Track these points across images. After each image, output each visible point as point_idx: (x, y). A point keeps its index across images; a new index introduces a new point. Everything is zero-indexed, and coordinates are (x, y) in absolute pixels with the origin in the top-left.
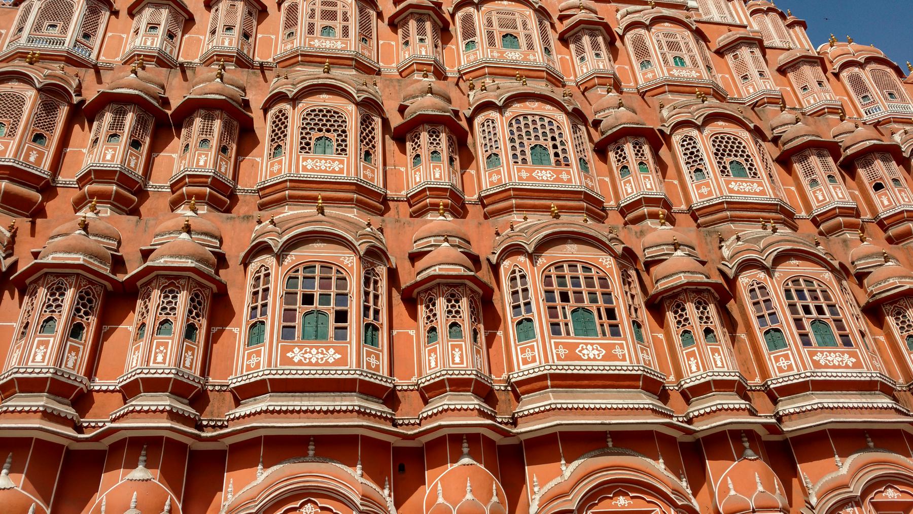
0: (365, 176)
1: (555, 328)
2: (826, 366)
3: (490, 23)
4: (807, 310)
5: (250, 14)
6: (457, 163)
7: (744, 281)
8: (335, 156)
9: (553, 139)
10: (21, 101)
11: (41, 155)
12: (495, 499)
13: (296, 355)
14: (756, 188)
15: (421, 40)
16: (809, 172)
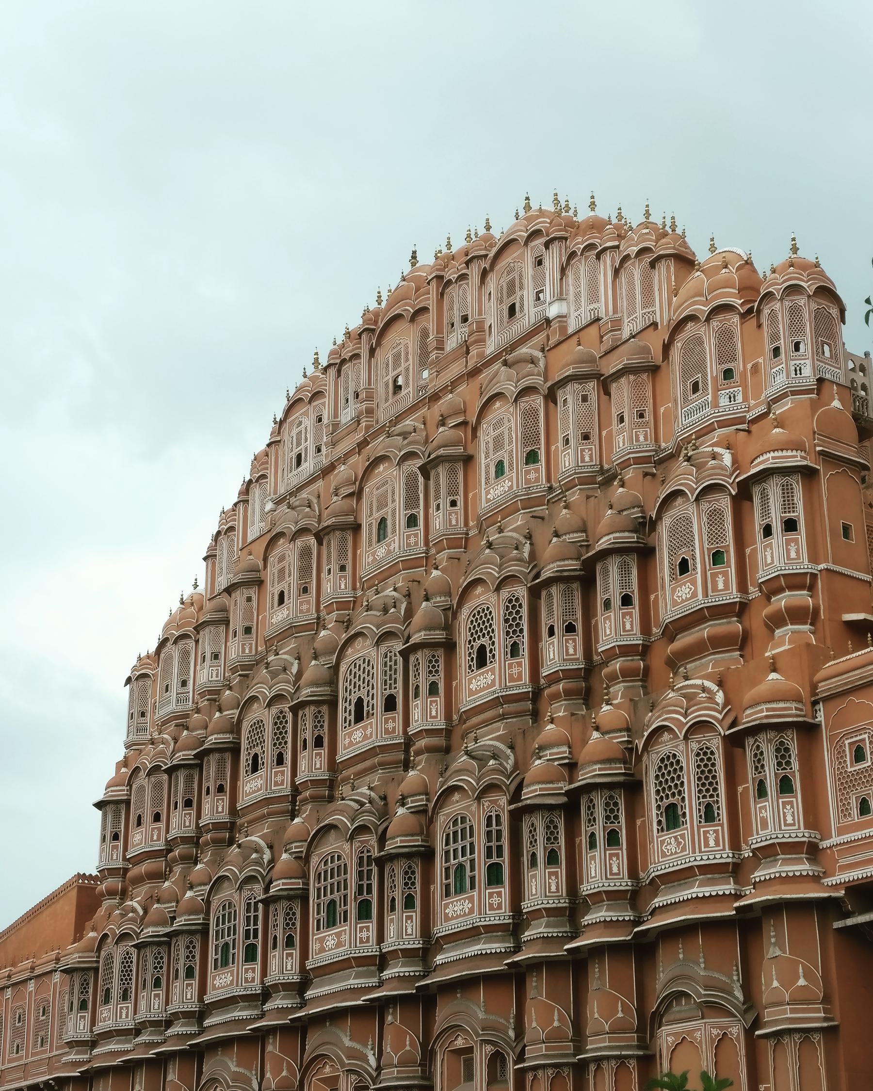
11: (159, 829)
12: (284, 1073)
14: (490, 677)
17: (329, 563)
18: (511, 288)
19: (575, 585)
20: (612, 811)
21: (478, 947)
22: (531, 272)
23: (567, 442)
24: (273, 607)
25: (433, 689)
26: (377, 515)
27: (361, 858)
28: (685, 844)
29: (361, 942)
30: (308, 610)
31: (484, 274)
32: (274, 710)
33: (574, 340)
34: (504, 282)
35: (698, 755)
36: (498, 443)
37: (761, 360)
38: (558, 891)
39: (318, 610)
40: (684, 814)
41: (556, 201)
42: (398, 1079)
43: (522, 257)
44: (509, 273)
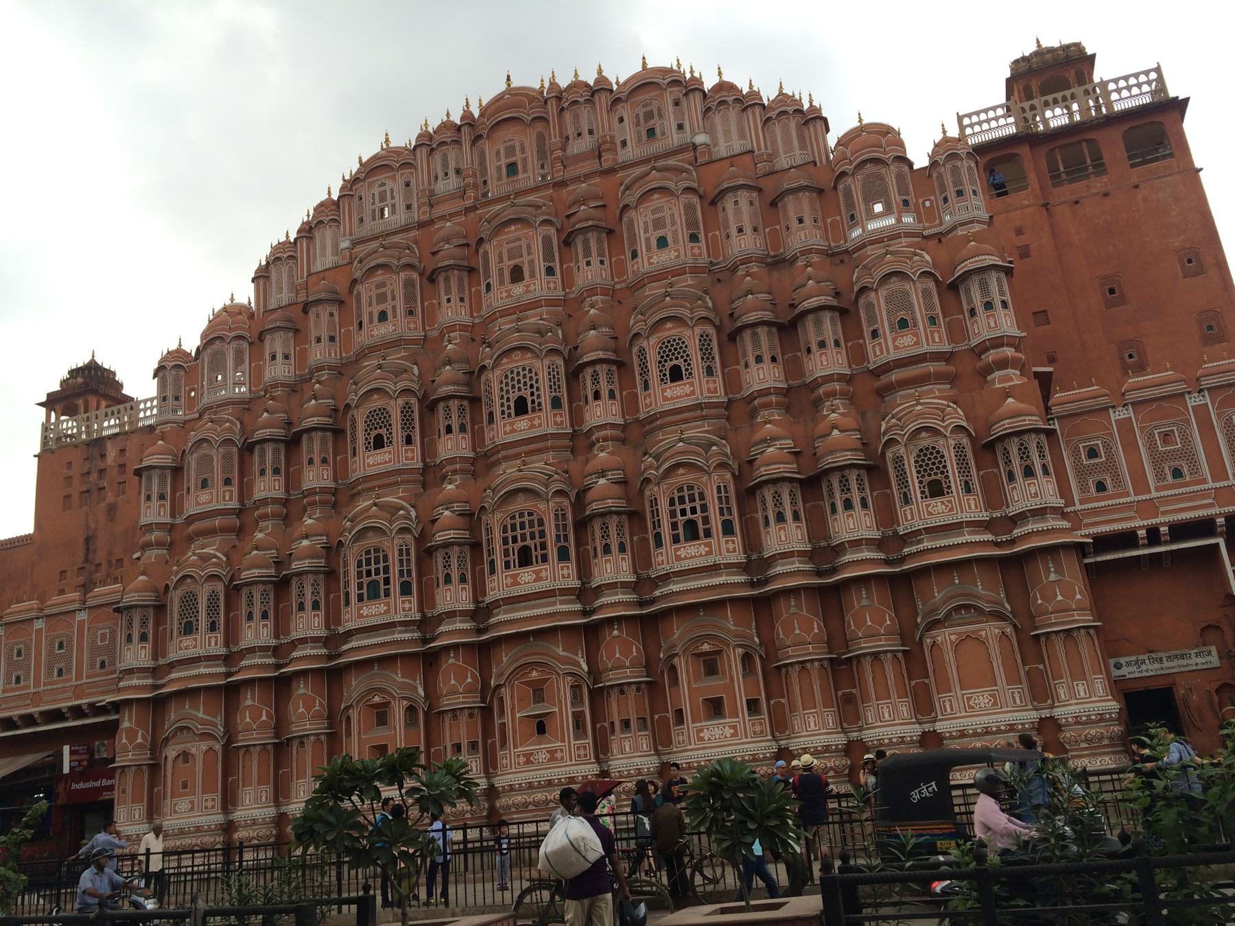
0: (407, 459)
1: (507, 566)
2: (686, 558)
3: (501, 261)
4: (683, 512)
5: (331, 315)
6: (469, 427)
7: (647, 493)
8: (386, 449)
9: (532, 386)
10: (211, 458)
11: (231, 492)
13: (365, 611)
14: (688, 389)
15: (449, 301)
16: (745, 355)
18: (649, 116)
19: (774, 329)
22: (671, 108)
23: (740, 230)
24: (371, 322)
26: (508, 264)
30: (416, 329)
31: (617, 101)
33: (727, 162)
34: (641, 111)
36: (659, 223)
37: (932, 198)
39: (424, 329)
40: (949, 487)
41: (679, 65)
43: (661, 96)
44: (644, 106)
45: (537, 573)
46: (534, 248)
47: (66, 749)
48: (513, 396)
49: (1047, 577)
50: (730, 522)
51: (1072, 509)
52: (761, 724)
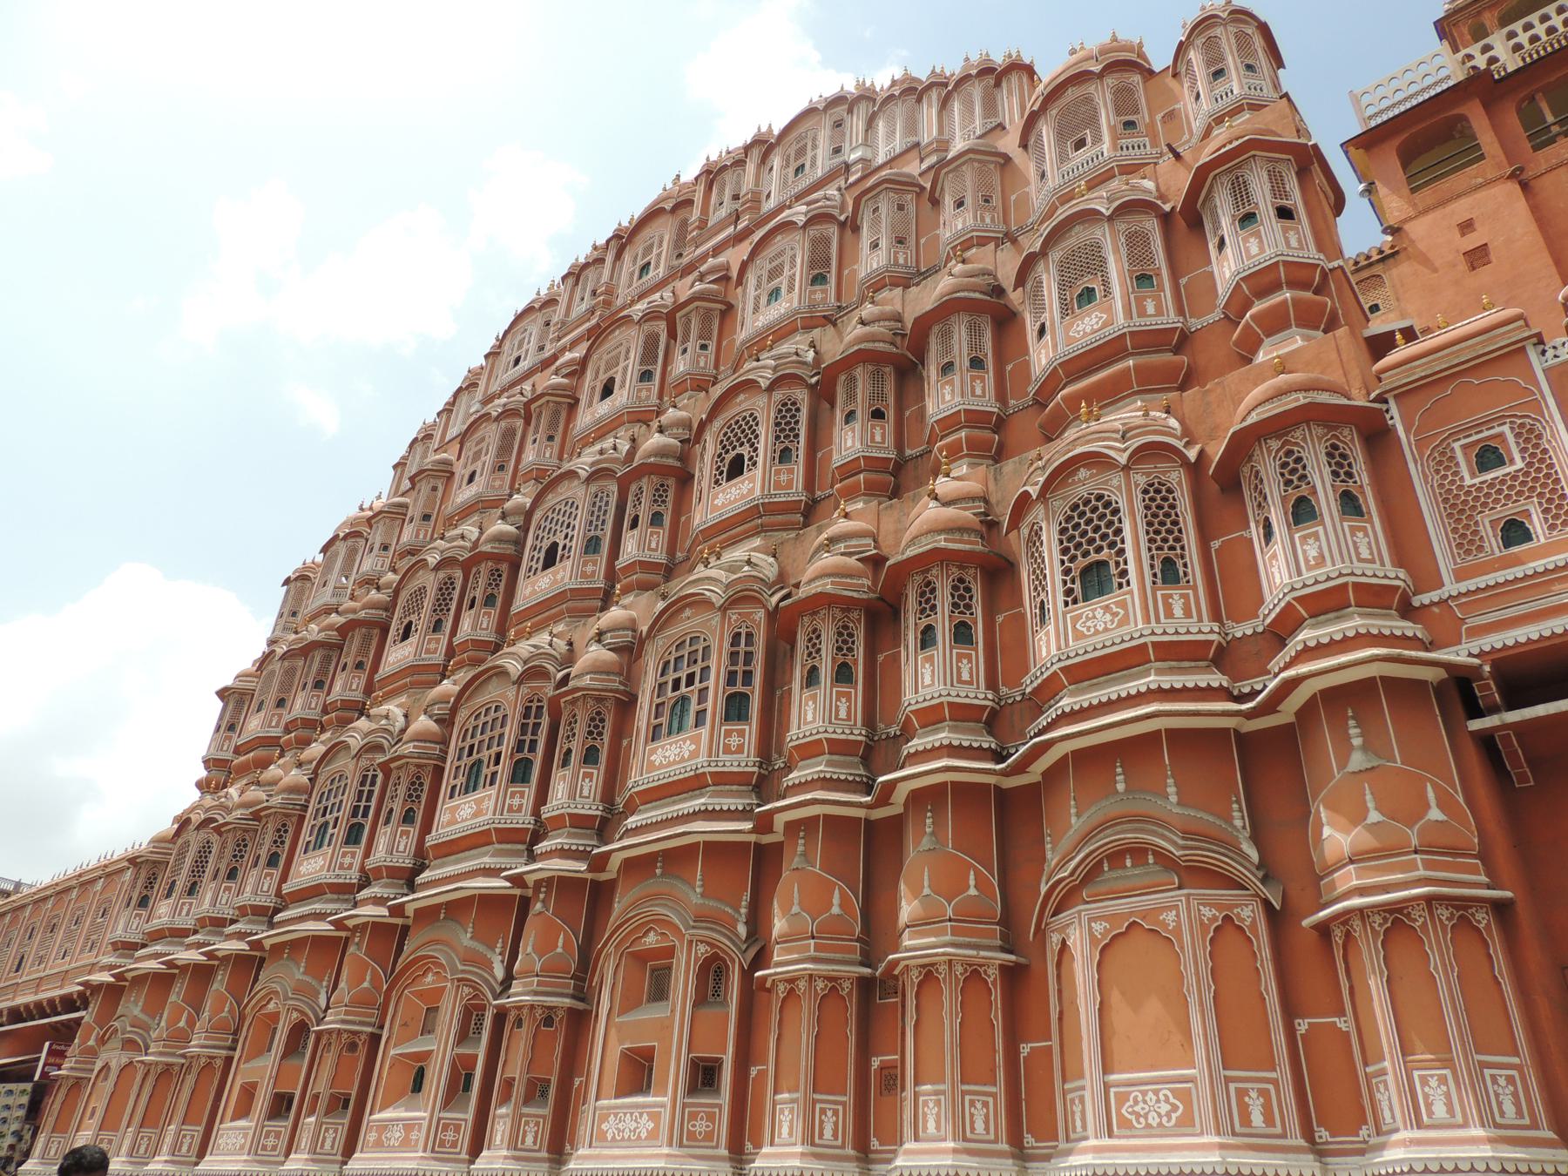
2: (661, 766)
12: (366, 985)
17: (536, 431)
18: (801, 152)
20: (962, 597)
21: (703, 800)
23: (875, 245)
25: (656, 519)
27: (528, 709)
28: (1127, 615)
29: (510, 810)
30: (501, 487)
32: (441, 575)
35: (1145, 492)
38: (849, 719)
40: (1124, 573)
42: (536, 993)
45: (479, 802)
46: (632, 355)
47: (47, 1044)
48: (546, 544)
49: (1343, 761)
50: (744, 698)
51: (1434, 596)
52: (711, 1117)
